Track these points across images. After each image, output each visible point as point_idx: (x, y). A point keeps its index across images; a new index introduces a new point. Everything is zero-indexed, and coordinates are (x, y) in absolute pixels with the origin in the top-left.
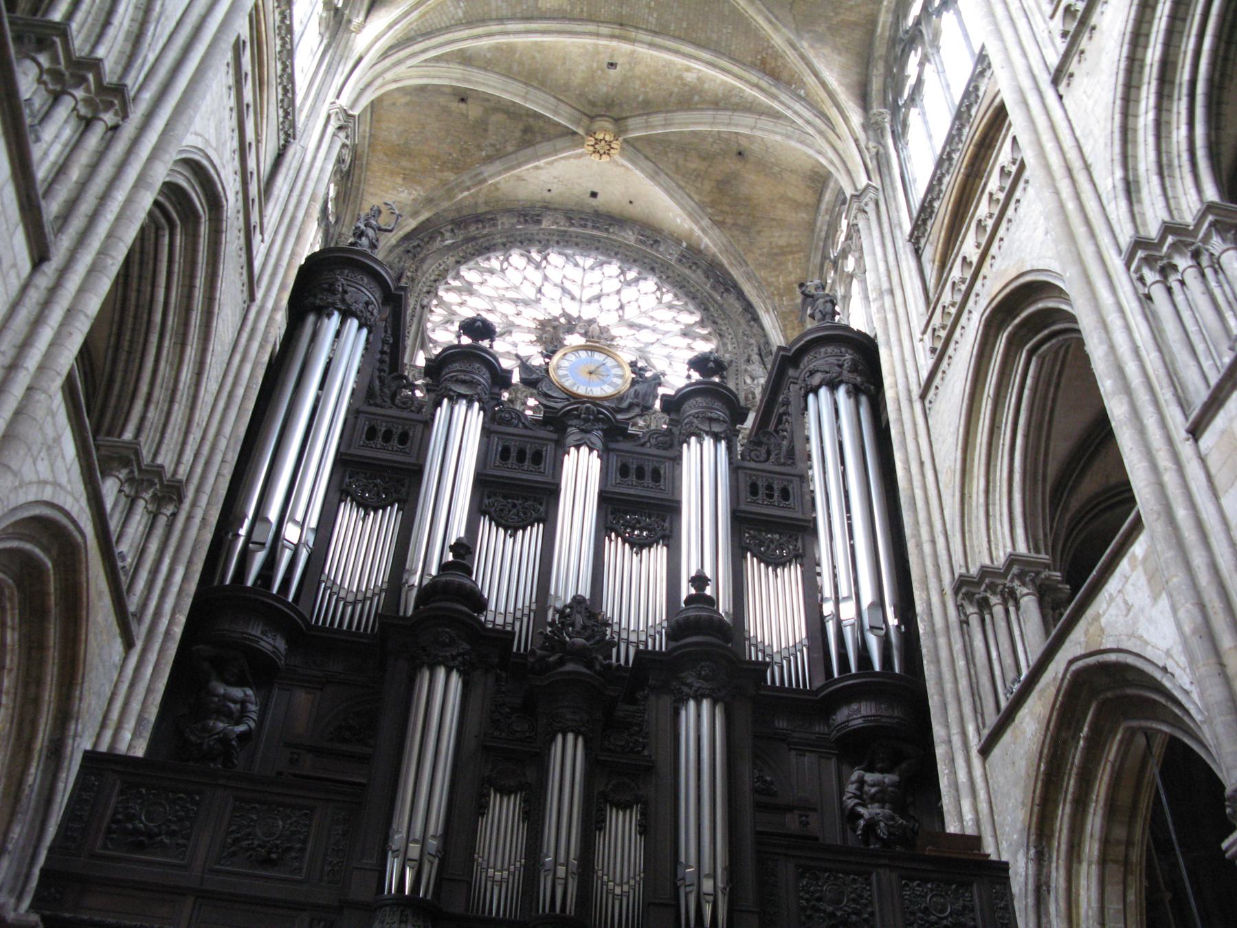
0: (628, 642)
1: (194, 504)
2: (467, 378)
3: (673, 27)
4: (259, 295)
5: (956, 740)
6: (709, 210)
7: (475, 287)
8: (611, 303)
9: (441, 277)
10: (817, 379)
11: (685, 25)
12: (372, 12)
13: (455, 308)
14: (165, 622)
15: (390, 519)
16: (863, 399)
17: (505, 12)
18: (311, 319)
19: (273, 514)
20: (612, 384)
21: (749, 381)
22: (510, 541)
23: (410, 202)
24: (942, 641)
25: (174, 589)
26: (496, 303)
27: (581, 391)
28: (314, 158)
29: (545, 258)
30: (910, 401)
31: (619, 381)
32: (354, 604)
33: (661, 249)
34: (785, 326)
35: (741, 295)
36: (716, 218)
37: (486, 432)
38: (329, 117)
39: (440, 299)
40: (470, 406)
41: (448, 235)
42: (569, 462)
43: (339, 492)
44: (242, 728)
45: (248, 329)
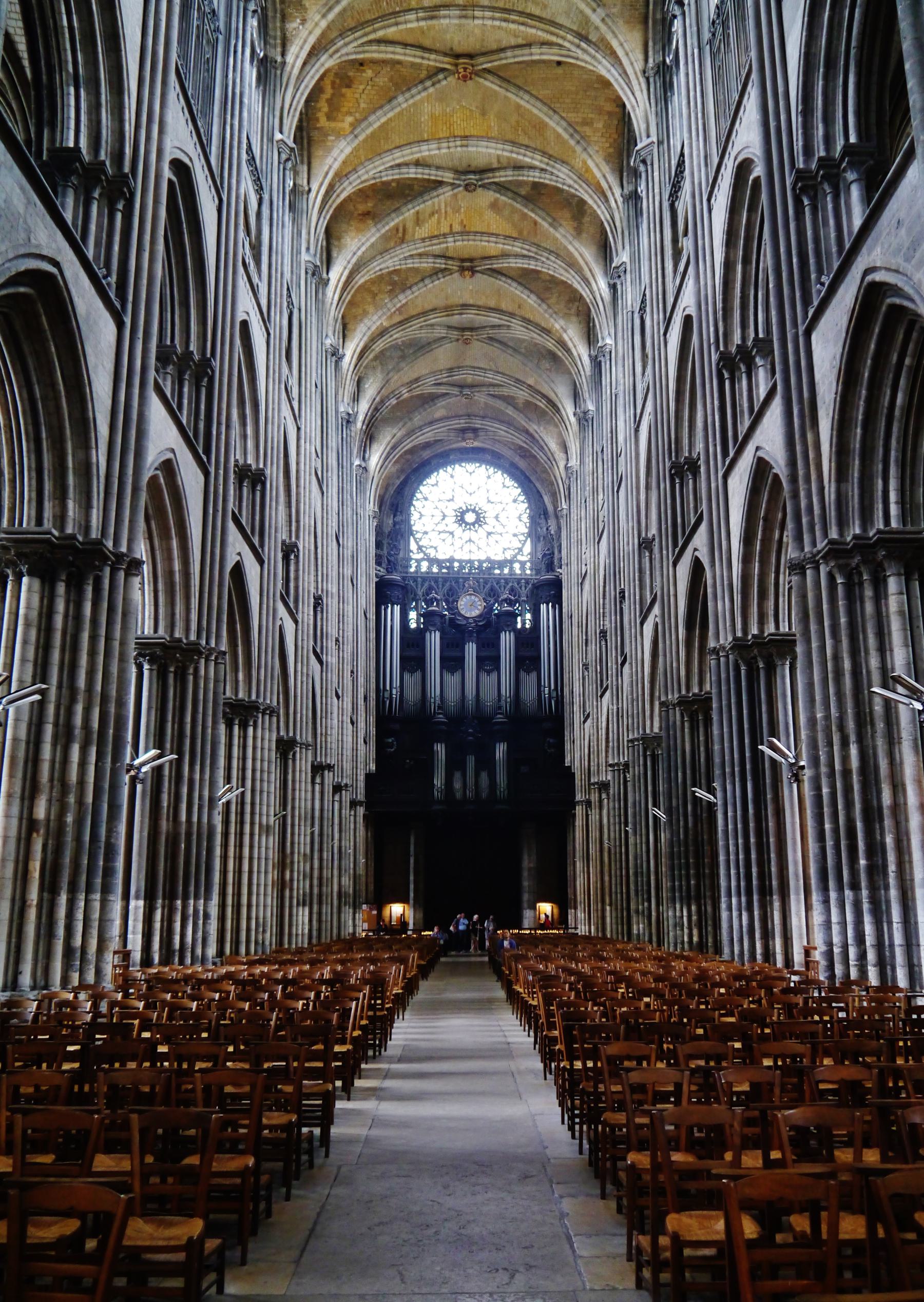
9: (413, 495)
13: (421, 510)
15: (418, 674)
17: (421, 423)
19: (388, 688)
27: (468, 615)
42: (467, 647)
43: (403, 669)
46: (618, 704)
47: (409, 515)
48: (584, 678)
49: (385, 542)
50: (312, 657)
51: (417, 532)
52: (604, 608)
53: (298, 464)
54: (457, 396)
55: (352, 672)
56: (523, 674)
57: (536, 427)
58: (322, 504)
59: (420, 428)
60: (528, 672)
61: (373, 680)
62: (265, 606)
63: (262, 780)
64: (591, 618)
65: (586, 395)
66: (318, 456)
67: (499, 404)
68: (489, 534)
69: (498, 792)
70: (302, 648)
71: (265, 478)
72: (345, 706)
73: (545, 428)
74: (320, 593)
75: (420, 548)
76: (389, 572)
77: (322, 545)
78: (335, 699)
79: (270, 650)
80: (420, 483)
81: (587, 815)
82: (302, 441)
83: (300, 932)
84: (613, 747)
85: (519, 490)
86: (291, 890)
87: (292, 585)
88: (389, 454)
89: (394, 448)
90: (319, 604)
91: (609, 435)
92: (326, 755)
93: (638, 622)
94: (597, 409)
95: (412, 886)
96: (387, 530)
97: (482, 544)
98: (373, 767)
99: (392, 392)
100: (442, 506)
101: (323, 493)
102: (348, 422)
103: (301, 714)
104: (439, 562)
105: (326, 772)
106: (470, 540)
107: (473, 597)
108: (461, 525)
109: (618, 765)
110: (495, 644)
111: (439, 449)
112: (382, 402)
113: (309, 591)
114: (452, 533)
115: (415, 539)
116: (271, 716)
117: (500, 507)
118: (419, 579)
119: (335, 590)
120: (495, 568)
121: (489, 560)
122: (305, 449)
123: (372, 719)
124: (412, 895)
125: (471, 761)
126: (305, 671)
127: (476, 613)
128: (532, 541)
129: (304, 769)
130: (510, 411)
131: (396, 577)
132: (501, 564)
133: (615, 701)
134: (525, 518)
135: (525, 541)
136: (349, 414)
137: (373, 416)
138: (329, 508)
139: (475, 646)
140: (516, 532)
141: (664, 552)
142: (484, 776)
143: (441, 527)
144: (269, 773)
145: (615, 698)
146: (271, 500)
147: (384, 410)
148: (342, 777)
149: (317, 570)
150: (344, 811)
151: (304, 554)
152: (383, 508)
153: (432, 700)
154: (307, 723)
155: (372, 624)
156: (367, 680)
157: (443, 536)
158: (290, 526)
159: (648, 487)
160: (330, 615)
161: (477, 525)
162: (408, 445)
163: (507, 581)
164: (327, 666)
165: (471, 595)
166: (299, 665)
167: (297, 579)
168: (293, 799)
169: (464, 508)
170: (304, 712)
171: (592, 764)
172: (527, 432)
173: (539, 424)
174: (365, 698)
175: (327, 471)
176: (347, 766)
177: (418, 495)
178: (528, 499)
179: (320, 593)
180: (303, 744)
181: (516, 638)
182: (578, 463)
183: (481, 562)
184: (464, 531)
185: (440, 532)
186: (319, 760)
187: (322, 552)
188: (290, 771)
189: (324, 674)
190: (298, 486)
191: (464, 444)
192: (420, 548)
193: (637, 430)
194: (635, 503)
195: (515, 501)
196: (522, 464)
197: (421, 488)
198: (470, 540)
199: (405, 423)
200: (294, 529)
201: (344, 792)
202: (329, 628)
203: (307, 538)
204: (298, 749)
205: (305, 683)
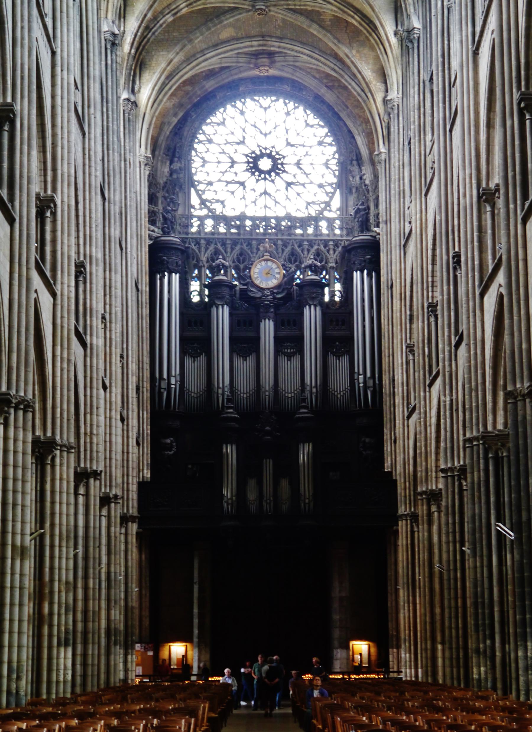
0: (288, 397)
1: (143, 387)
2: (220, 296)
3: (289, 35)
4: (140, 287)
5: (389, 436)
6: (325, 81)
7: (212, 137)
8: (281, 130)
9: (194, 137)
10: (356, 268)
11: (295, 34)
12: (142, 73)
13: (204, 155)
14: (145, 432)
15: (203, 359)
16: (374, 274)
17: (204, 46)
18: (158, 276)
19: (165, 376)
20: (276, 279)
21: (351, 179)
22: (245, 362)
23: (171, 107)
24: (388, 399)
25: (145, 420)
26: (223, 147)
27: (263, 285)
28: (141, 199)
29: (244, 104)
30: (388, 287)
31: (278, 276)
32: (197, 398)
33: (304, 93)
34: (369, 142)
35: (345, 124)
36: (330, 84)
37: (231, 314)
38: (140, 162)
39: (195, 150)
40: (223, 308)
41: (193, 114)
42: (262, 325)
43: (183, 352)
44: (172, 452)
45: (140, 306)
46: (451, 395)
47: (189, 161)
48: (408, 363)
49: (160, 195)
50: (74, 339)
51: (200, 182)
52: (433, 276)
53: (53, 97)
54: (249, 11)
55: (122, 357)
56: (332, 359)
57: (347, 51)
58: (84, 149)
59: (203, 52)
60: (338, 356)
61: (147, 367)
62: (16, 276)
63: (15, 491)
64: (417, 288)
65: (411, 9)
66: (77, 88)
67: (302, 21)
68: (289, 184)
69: (302, 505)
70: (62, 327)
71: (14, 115)
72: (113, 399)
73: (358, 52)
74: (82, 258)
75: (203, 202)
76: (165, 232)
77: (84, 199)
78: (102, 391)
79: (23, 330)
80: (203, 121)
81: (412, 532)
82: (58, 69)
83: (61, 678)
84: (446, 448)
85: (326, 130)
86: (51, 626)
87: (48, 249)
88: (164, 85)
89: (170, 77)
90: (81, 272)
91: (440, 60)
92: (91, 459)
93: (477, 293)
94: (425, 27)
95: (196, 621)
96: (161, 181)
97: (280, 197)
98: (147, 474)
99: (168, 6)
100: (229, 149)
101: (84, 134)
102: (113, 44)
103: (62, 410)
104: (226, 220)
105: (92, 480)
106: (265, 193)
107: (270, 264)
108: (253, 174)
109: (451, 469)
110: (299, 322)
111: (226, 78)
112: (155, 18)
113: (69, 257)
114: (242, 184)
115: (197, 191)
116: (25, 412)
117: (301, 151)
118: (203, 241)
119: (100, 256)
120: (296, 228)
121: (289, 217)
122: (62, 79)
123: (146, 415)
124: (196, 631)
125: (268, 466)
126: (65, 355)
127: (273, 283)
128: (341, 194)
129: (65, 476)
130: (314, 30)
131: (174, 238)
132: (304, 222)
133: (447, 392)
134: (334, 164)
135: (333, 194)
136: (114, 35)
137: (143, 37)
138: (92, 153)
139: (272, 323)
140: (323, 182)
141: (512, 206)
142: (284, 483)
143: (229, 177)
144: (24, 481)
145: (447, 387)
146: (22, 144)
147: (158, 30)
148: (111, 486)
149: (78, 231)
150: (113, 529)
151: (62, 211)
152: (157, 153)
153: (220, 391)
154: (68, 420)
155: (145, 298)
156: (140, 368)
157: (232, 187)
158: (45, 175)
159: (490, 125)
160: (94, 286)
161: (273, 174)
162: (188, 73)
163: (311, 243)
164: (91, 349)
165: (267, 260)
166: (59, 348)
167: (54, 241)
168: (53, 514)
169: (258, 153)
170: (65, 407)
171: (419, 469)
172: (336, 56)
173: (350, 45)
174: (138, 389)
175: (89, 107)
176: (117, 473)
177: (201, 137)
178: (337, 141)
179: (82, 258)
180: (65, 446)
181: (324, 314)
182: (400, 95)
183: (278, 219)
184: (257, 181)
185: (228, 183)
186: (82, 465)
187: (84, 208)
188: (48, 479)
189: (88, 359)
190: (54, 126)
191: (256, 72)
192: (203, 202)
193: (476, 53)
194: (473, 144)
195: (320, 143)
196: (329, 97)
197: (204, 127)
198: (265, 193)
199: (184, 46)
200: (49, 179)
201: (113, 505)
202: (94, 302)
203: (66, 190)
204: (58, 452)
205: (65, 371)
